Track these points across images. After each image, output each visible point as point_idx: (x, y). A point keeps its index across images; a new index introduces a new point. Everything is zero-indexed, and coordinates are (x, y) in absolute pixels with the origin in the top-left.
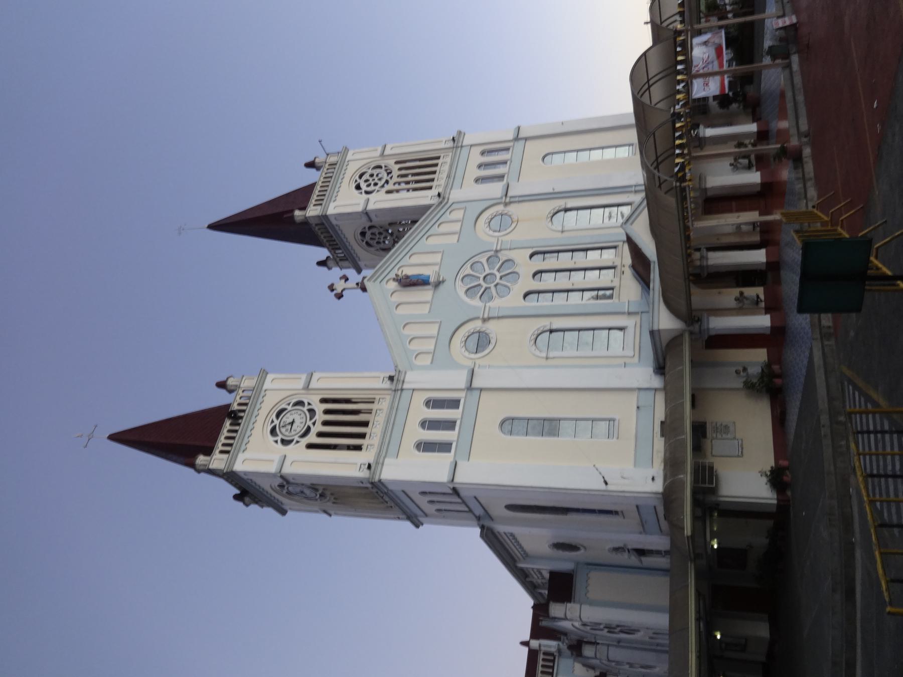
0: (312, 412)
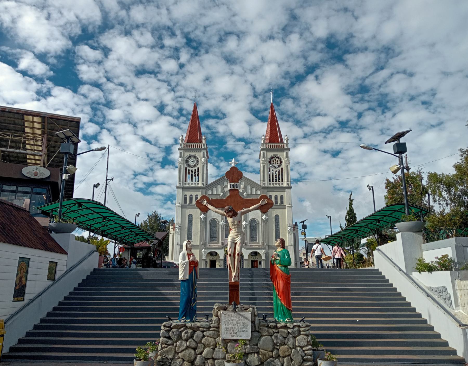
0: (195, 166)
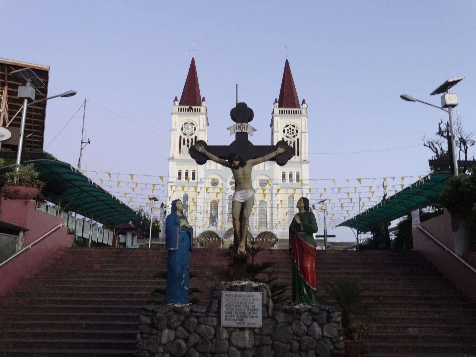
0: (192, 134)
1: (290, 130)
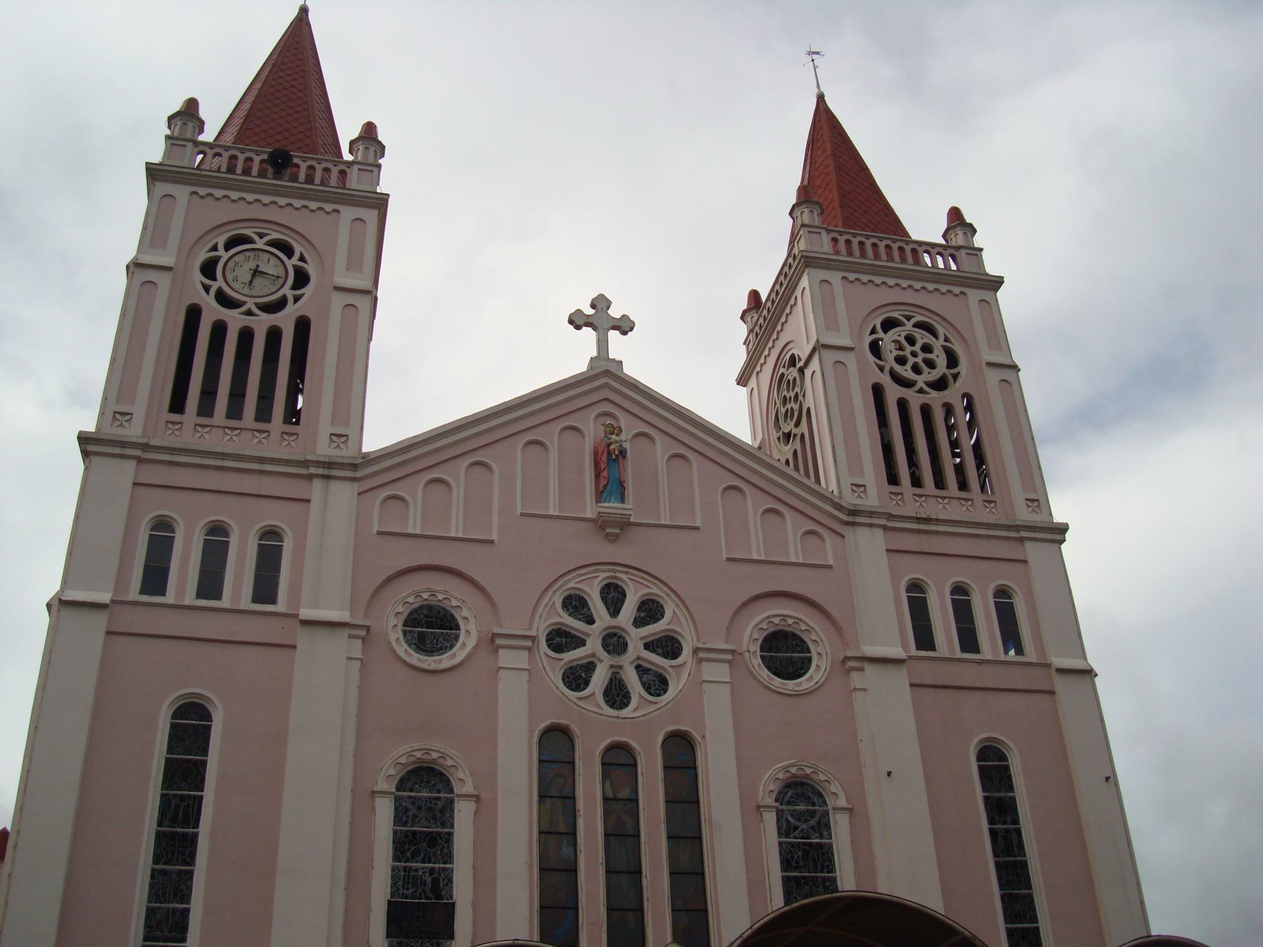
1: (909, 349)
